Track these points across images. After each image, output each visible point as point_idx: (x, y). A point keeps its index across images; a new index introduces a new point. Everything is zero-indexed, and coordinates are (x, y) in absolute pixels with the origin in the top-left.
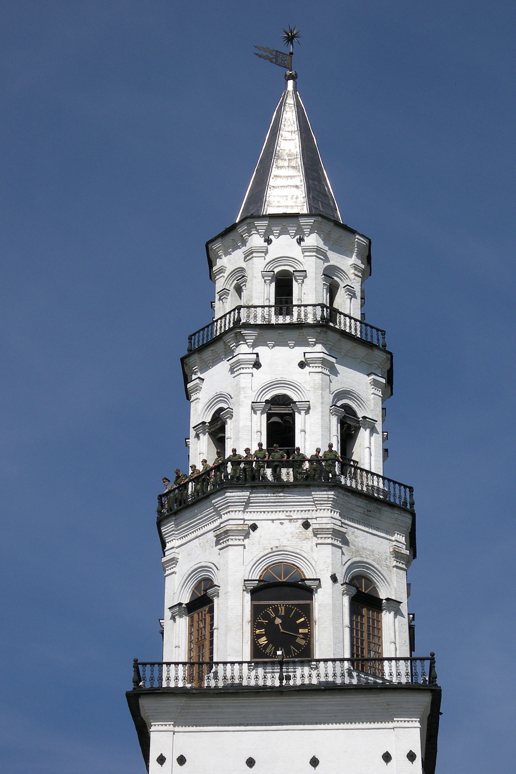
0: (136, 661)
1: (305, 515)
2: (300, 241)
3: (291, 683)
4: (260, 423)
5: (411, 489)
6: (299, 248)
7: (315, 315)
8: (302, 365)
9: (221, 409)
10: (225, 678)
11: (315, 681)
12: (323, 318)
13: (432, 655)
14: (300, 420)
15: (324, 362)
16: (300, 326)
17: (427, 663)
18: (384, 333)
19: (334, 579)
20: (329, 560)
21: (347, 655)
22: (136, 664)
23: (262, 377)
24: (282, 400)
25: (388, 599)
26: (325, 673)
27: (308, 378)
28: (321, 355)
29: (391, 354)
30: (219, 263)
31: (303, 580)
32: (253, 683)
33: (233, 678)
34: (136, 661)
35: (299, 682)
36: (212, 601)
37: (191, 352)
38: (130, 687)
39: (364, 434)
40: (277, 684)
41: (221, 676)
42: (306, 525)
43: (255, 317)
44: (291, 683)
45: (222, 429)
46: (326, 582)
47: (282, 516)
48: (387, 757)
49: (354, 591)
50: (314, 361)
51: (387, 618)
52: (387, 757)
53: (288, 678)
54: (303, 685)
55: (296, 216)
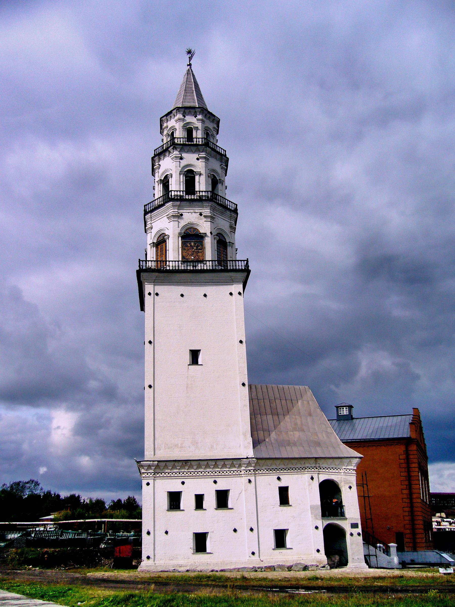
0: (139, 259)
1: (201, 211)
2: (196, 117)
3: (197, 268)
4: (182, 178)
5: (237, 205)
6: (195, 119)
7: (202, 142)
8: (198, 159)
9: (168, 175)
10: (172, 266)
11: (205, 268)
12: (205, 142)
13: (248, 259)
14: (197, 178)
15: (205, 158)
16: (197, 145)
17: (246, 262)
18: (225, 151)
19: (211, 233)
20: (210, 227)
21: (216, 259)
22: (140, 260)
23: (183, 163)
24: (191, 171)
25: (229, 242)
26: (209, 266)
27: (200, 164)
28: (205, 156)
29: (228, 158)
30: (165, 125)
31: (200, 233)
32: (183, 268)
33: (175, 266)
34: (139, 259)
35: (199, 268)
36: (166, 241)
37: (155, 156)
38: (138, 269)
39: (220, 186)
40: (192, 268)
41: (171, 266)
42: (201, 214)
43: (180, 141)
44: (197, 268)
45: (168, 182)
46: (209, 234)
47: (192, 211)
48: (231, 294)
49: (218, 238)
50: (201, 158)
51: (229, 249)
52: (231, 294)
53: (196, 267)
54: (201, 269)
55: (194, 108)
